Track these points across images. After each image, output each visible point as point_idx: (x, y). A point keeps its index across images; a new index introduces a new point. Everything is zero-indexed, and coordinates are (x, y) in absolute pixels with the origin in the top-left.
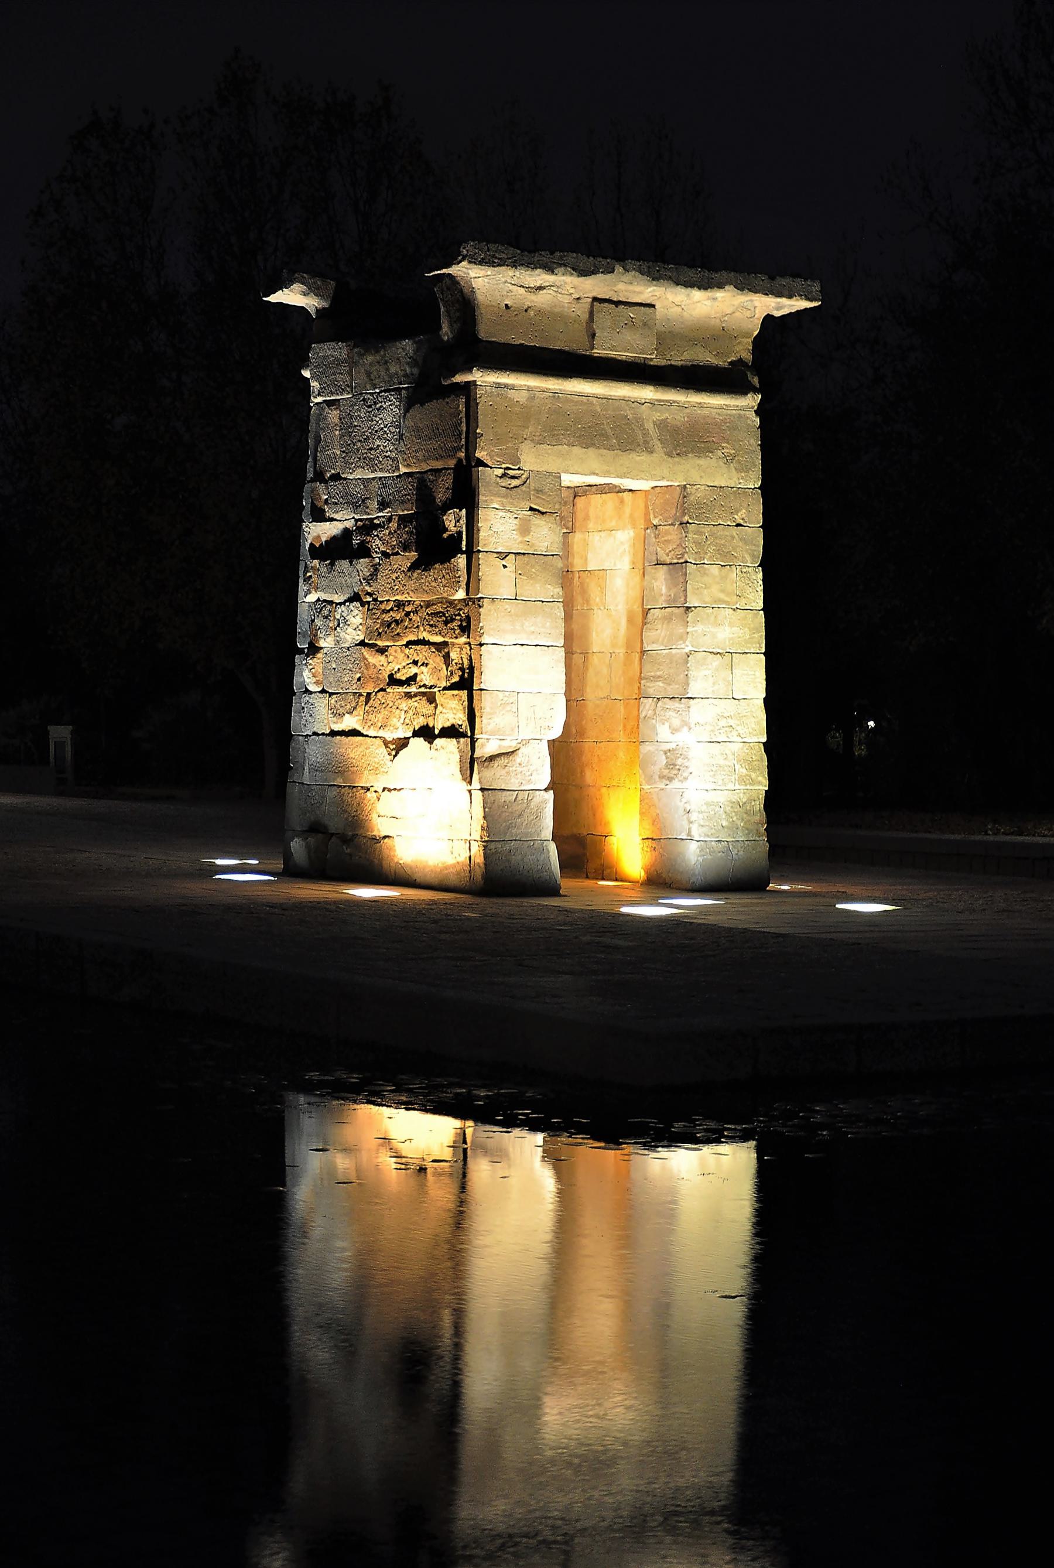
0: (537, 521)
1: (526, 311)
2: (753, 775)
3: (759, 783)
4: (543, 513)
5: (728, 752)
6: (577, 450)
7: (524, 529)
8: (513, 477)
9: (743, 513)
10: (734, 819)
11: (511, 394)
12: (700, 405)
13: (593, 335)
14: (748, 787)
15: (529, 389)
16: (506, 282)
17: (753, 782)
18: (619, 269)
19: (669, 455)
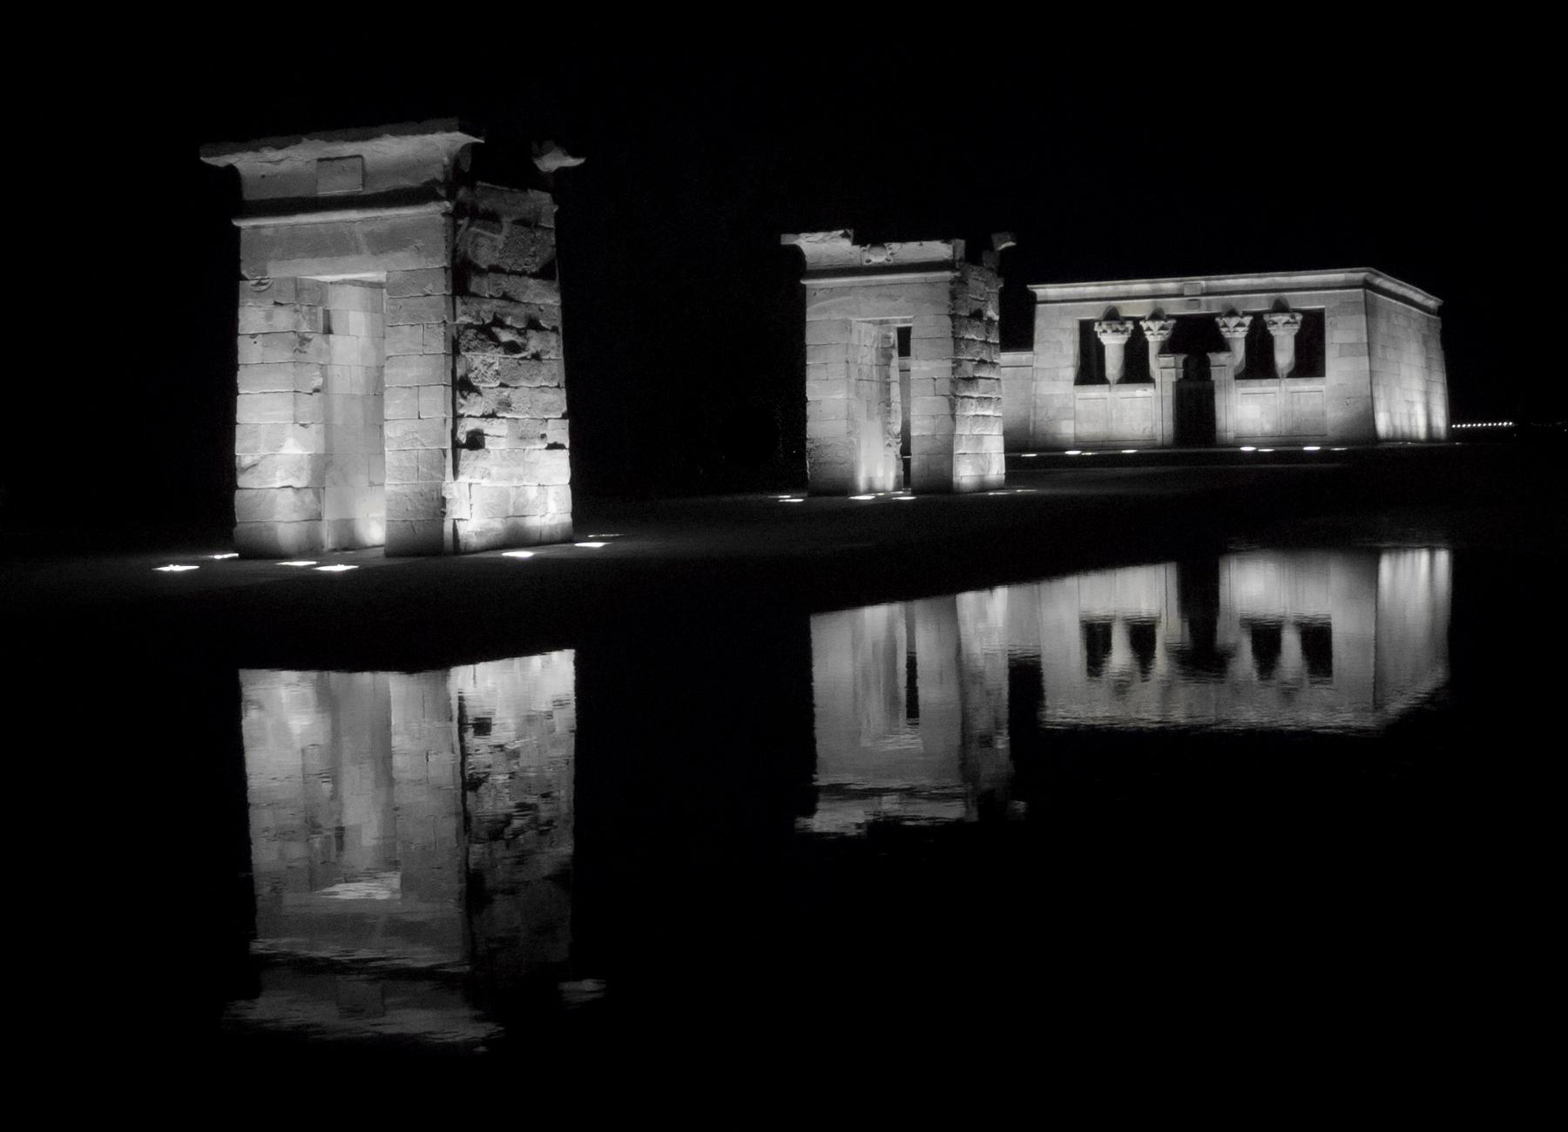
0: (279, 310)
1: (276, 176)
2: (433, 472)
3: (439, 479)
4: (282, 304)
5: (413, 457)
6: (306, 261)
7: (269, 317)
8: (265, 284)
9: (430, 286)
10: (417, 504)
11: (264, 232)
12: (399, 216)
13: (317, 182)
14: (429, 482)
15: (275, 226)
16: (255, 162)
17: (432, 478)
18: (304, 139)
19: (374, 254)
